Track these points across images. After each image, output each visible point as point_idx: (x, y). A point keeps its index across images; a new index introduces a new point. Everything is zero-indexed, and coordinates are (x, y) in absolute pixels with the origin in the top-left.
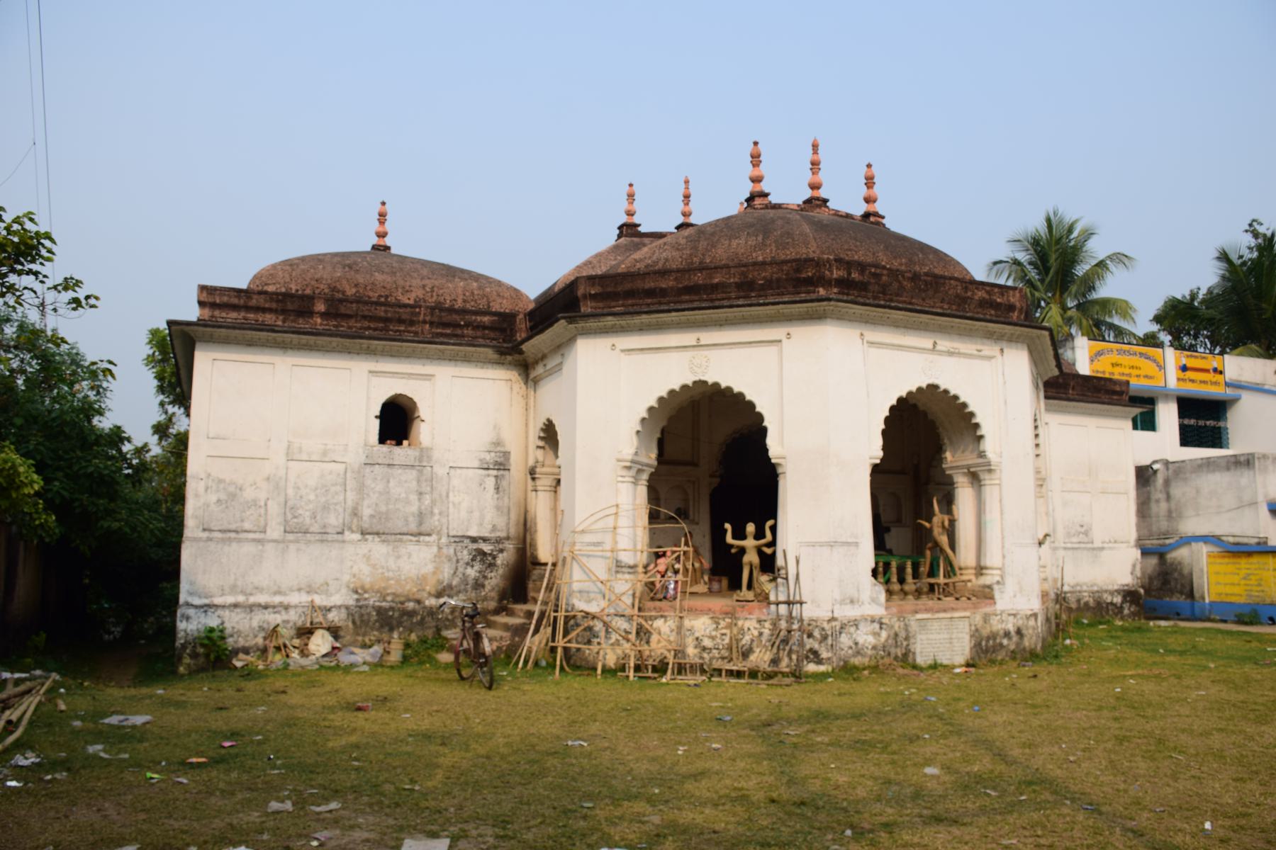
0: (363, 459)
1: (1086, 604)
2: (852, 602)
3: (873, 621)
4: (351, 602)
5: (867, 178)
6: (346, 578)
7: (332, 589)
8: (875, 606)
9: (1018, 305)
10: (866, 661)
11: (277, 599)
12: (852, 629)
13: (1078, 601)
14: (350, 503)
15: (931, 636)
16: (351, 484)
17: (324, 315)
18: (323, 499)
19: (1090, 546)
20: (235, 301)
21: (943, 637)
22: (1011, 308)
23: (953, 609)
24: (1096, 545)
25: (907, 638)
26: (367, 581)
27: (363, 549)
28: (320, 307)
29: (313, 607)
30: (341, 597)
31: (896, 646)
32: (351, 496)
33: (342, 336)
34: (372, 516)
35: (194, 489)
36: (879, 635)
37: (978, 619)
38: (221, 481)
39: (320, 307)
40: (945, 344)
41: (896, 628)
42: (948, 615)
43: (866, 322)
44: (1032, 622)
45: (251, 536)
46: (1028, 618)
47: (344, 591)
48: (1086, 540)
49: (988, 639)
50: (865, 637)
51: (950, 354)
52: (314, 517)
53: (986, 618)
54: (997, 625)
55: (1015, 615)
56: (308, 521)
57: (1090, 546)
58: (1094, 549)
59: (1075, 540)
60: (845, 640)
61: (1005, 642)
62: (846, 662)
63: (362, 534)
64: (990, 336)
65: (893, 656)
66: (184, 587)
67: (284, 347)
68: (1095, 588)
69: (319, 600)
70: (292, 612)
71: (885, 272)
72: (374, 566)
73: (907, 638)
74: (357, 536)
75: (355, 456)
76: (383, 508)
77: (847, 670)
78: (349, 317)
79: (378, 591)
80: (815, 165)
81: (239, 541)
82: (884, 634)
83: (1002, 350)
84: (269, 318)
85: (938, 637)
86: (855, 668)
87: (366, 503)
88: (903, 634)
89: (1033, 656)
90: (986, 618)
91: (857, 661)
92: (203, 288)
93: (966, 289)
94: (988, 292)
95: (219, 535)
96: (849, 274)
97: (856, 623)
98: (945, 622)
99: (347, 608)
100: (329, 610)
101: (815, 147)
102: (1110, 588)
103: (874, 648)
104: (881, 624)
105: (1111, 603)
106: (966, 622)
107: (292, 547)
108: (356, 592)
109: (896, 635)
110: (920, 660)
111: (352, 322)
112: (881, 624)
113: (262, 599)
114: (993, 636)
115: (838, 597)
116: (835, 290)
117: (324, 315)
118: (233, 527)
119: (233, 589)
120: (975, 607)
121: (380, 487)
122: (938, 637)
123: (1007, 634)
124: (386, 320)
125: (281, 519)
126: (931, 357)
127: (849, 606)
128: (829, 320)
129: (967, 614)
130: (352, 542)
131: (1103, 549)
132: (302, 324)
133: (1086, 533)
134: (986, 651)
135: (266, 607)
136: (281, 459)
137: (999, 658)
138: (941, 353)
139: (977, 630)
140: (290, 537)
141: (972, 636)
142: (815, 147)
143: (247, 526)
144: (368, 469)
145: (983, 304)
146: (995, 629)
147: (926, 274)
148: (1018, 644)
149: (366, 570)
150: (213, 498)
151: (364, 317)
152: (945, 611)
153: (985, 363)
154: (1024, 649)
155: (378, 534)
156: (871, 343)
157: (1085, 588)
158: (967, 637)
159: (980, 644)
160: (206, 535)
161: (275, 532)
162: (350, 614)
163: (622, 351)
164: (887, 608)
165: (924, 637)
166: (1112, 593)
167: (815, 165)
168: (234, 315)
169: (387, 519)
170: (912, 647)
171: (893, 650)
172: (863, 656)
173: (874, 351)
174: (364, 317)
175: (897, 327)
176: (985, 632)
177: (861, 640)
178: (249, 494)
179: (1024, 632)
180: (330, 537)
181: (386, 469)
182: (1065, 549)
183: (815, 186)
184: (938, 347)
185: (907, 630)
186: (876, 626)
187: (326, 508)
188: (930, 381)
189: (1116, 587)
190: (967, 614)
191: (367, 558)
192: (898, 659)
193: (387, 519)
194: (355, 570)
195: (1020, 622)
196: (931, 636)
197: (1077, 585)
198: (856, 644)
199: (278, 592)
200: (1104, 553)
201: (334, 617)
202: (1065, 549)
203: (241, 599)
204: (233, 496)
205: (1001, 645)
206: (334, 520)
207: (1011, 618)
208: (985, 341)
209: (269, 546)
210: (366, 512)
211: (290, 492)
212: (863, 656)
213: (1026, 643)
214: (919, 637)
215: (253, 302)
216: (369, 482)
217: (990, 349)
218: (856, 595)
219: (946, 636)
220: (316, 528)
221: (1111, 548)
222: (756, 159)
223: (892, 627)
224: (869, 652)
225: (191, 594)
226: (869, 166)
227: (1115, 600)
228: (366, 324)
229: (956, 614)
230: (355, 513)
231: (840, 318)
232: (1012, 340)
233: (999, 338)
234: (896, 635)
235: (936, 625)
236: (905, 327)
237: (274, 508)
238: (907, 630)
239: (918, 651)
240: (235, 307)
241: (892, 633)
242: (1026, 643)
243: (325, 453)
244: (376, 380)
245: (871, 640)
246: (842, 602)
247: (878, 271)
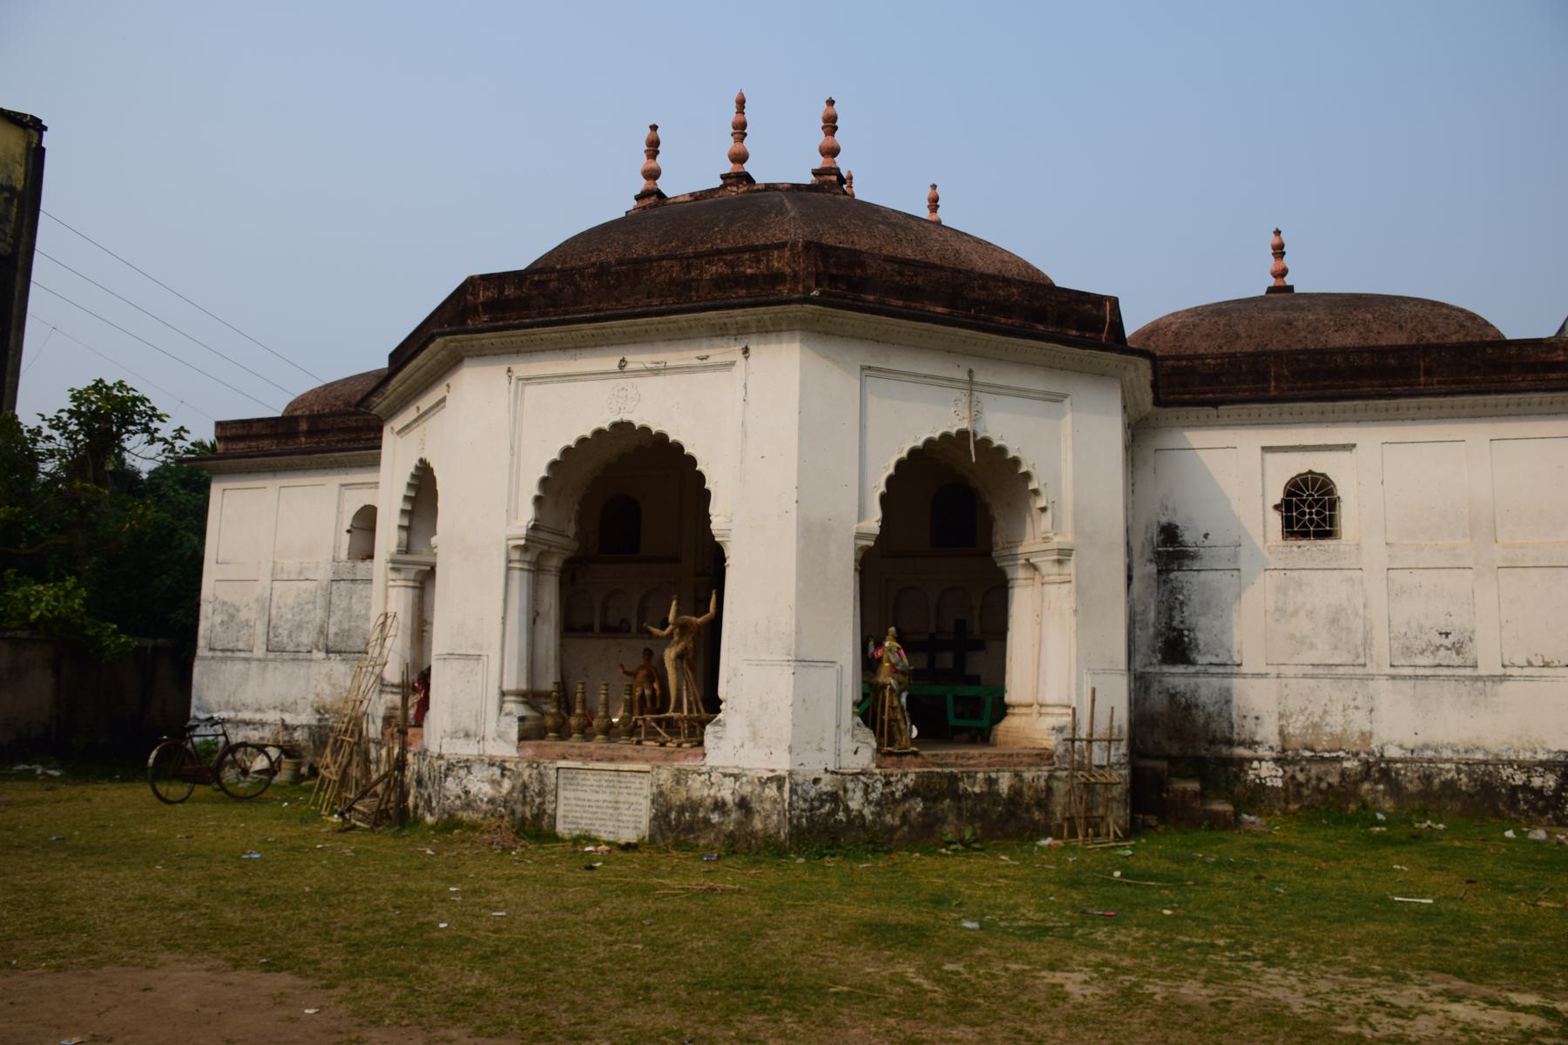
0: (330, 576)
1: (1449, 785)
2: (467, 735)
3: (492, 765)
4: (314, 722)
5: (825, 120)
6: (311, 697)
7: (300, 708)
8: (502, 744)
9: (788, 270)
10: (477, 816)
11: (258, 716)
12: (462, 773)
13: (1427, 778)
14: (318, 621)
15: (581, 795)
16: (320, 602)
17: (308, 433)
18: (298, 618)
19: (1468, 672)
20: (240, 432)
21: (606, 798)
22: (776, 278)
23: (626, 758)
24: (1481, 671)
25: (541, 793)
26: (328, 700)
27: (325, 668)
28: (304, 426)
29: (285, 727)
30: (306, 717)
31: (524, 803)
32: (319, 614)
33: (323, 451)
34: (336, 634)
35: (206, 609)
36: (499, 784)
37: (665, 776)
38: (224, 603)
39: (304, 426)
40: (639, 359)
41: (526, 777)
42: (612, 766)
43: (518, 352)
44: (771, 791)
45: (242, 655)
46: (763, 783)
47: (309, 710)
48: (1457, 660)
49: (682, 809)
50: (480, 785)
51: (655, 372)
52: (290, 636)
53: (680, 778)
54: (697, 788)
55: (736, 777)
56: (285, 640)
57: (1468, 672)
58: (1478, 678)
59: (1420, 660)
60: (451, 785)
61: (715, 818)
62: (451, 816)
63: (327, 652)
64: (720, 332)
65: (519, 815)
66: (194, 702)
67: (274, 470)
68: (1480, 756)
69: (290, 719)
70: (267, 729)
71: (554, 276)
72: (333, 686)
73: (541, 793)
74: (322, 655)
75: (324, 573)
76: (346, 626)
77: (450, 824)
78: (325, 432)
79: (337, 712)
80: (740, 130)
81: (233, 659)
82: (507, 784)
83: (746, 351)
84: (266, 444)
85: (594, 797)
86: (459, 824)
87: (332, 620)
88: (535, 787)
89: (770, 849)
90: (680, 778)
91: (466, 816)
92: (219, 425)
93: (689, 267)
94: (731, 264)
95: (219, 654)
96: (501, 291)
97: (467, 765)
98: (606, 775)
99: (309, 727)
100: (295, 728)
101: (741, 103)
102: (1526, 756)
103: (491, 801)
104: (504, 769)
105: (1526, 787)
106: (647, 779)
107: (271, 666)
108: (318, 712)
109: (525, 787)
110: (561, 828)
111: (330, 437)
112: (504, 769)
113: (246, 715)
114: (693, 806)
115: (449, 730)
116: (485, 318)
117: (308, 433)
118: (230, 646)
119: (228, 705)
120: (668, 758)
121: (343, 604)
122: (594, 797)
123: (719, 806)
124: (357, 430)
125: (264, 639)
126: (621, 382)
127: (462, 741)
128: (466, 361)
129: (647, 767)
130: (317, 661)
131: (1504, 678)
132: (291, 446)
133: (1458, 648)
134: (677, 826)
135: (247, 723)
136: (267, 581)
137: (702, 842)
138: (637, 373)
139: (661, 794)
140: (271, 656)
141: (653, 802)
142: (741, 103)
143: (241, 645)
144: (335, 585)
145: (720, 283)
146: (695, 795)
147: (620, 262)
148: (740, 824)
149: (327, 689)
150: (218, 619)
151: (339, 430)
152: (612, 760)
153: (722, 375)
154: (753, 834)
155: (340, 652)
156: (528, 379)
157: (1447, 754)
158: (646, 803)
159: (666, 816)
160: (210, 654)
161: (259, 651)
162: (311, 734)
163: (399, 432)
164: (519, 748)
165: (570, 794)
166: (1527, 767)
167: (740, 130)
168: (241, 445)
169: (349, 637)
170: (549, 808)
171: (519, 808)
172: (477, 810)
173: (531, 391)
174: (339, 430)
175: (564, 349)
176: (679, 798)
177: (473, 788)
178: (243, 615)
179: (755, 805)
180: (300, 656)
181: (350, 585)
182: (1393, 677)
183: (739, 158)
184: (629, 367)
185: (541, 782)
186: (497, 771)
187: (300, 627)
188: (617, 419)
189: (1542, 756)
190: (647, 767)
191: (329, 676)
192: (530, 825)
193: (349, 637)
194: (318, 690)
195: (747, 789)
196: (581, 795)
197: (1426, 747)
198: (467, 793)
199: (259, 710)
200: (1507, 684)
201: (298, 735)
202: (1393, 677)
203: (231, 715)
204: (232, 617)
205: (707, 821)
206: (306, 638)
207: (729, 782)
208: (717, 341)
209: (254, 664)
210: (332, 630)
211: (273, 611)
212: (477, 810)
213: (758, 824)
214: (562, 794)
215: (254, 431)
216: (334, 599)
217: (720, 352)
218: (472, 727)
219: (609, 798)
220: (290, 647)
221: (1530, 678)
222: (653, 147)
223: (520, 775)
224: (484, 806)
225: (198, 709)
226: (831, 102)
227: (1537, 782)
228: (341, 436)
229: (626, 767)
230: (322, 632)
231: (481, 354)
232: (767, 330)
233: (742, 331)
234: (525, 787)
235: (591, 779)
236: (576, 347)
237: (260, 629)
238: (541, 782)
239: (560, 813)
240: (241, 438)
241: (519, 783)
242: (758, 824)
243: (300, 573)
244: (348, 493)
245: (488, 790)
246: (454, 735)
247: (544, 277)
